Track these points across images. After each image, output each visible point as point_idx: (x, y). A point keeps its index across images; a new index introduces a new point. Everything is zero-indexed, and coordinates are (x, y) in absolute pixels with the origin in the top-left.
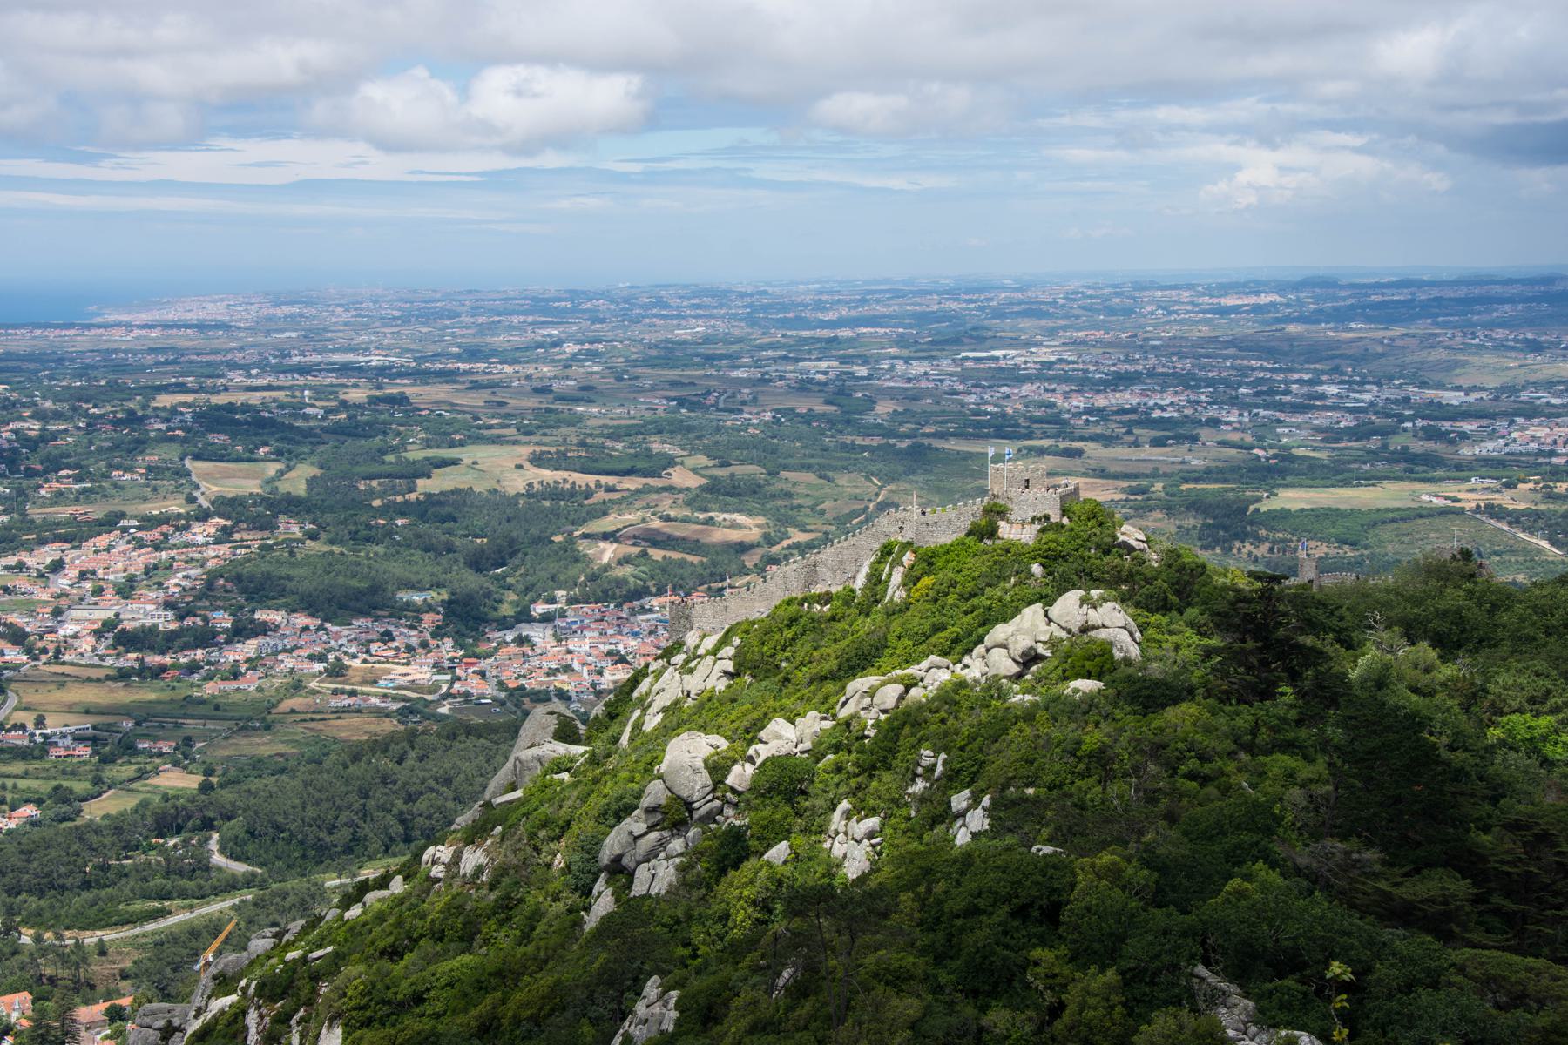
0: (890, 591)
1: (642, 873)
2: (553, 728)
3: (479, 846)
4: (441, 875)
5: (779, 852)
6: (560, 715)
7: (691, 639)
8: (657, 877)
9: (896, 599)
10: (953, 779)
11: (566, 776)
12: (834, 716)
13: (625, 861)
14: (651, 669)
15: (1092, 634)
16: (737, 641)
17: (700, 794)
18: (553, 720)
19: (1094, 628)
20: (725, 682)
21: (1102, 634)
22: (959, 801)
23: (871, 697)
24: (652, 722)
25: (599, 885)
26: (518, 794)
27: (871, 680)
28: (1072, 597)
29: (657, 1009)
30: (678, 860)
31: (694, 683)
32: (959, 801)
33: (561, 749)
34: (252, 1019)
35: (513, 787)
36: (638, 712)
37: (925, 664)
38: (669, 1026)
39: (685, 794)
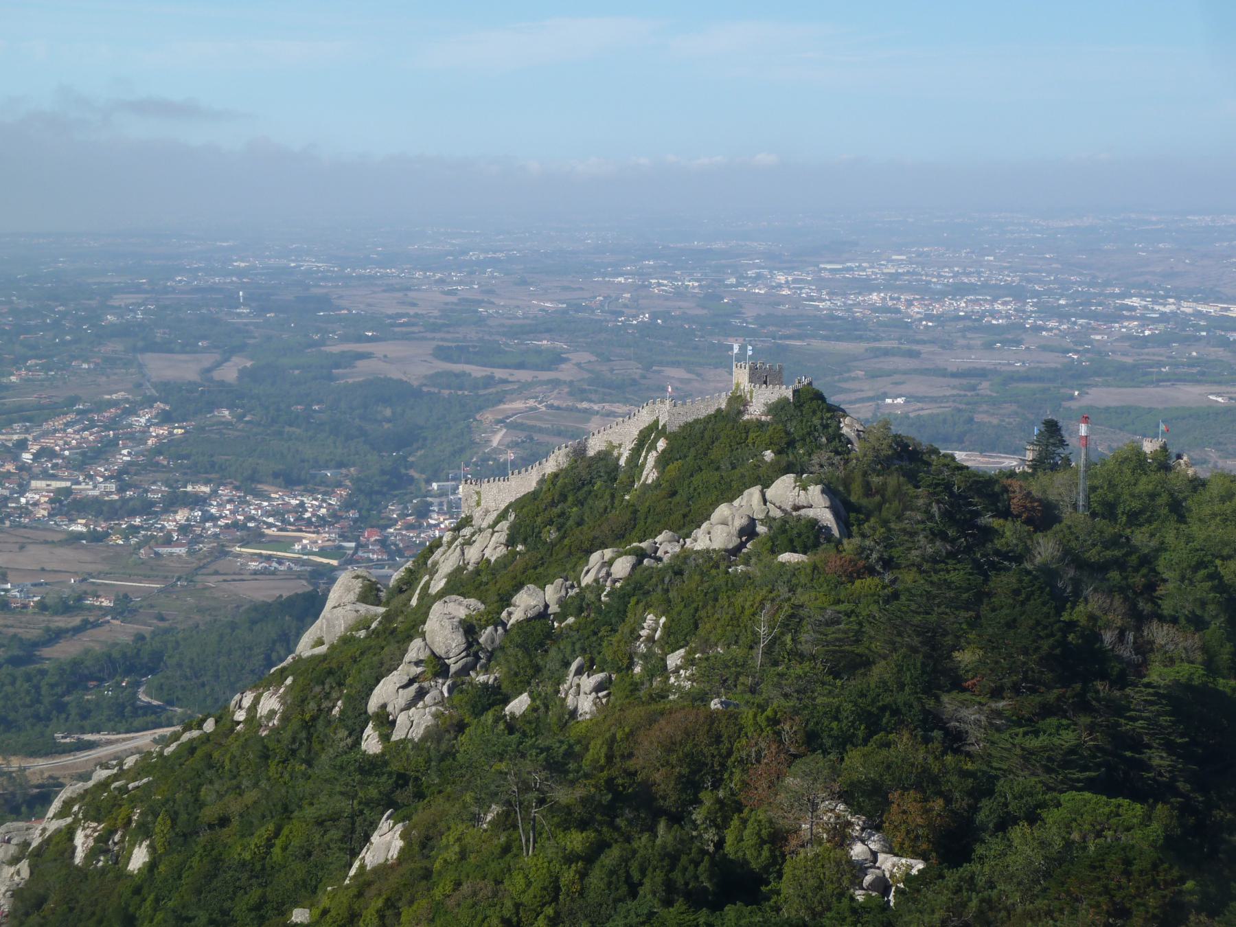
0: (645, 473)
1: (402, 719)
2: (357, 590)
3: (274, 694)
4: (242, 718)
5: (519, 704)
6: (364, 578)
7: (477, 513)
8: (414, 723)
9: (649, 481)
10: (672, 639)
11: (362, 634)
12: (579, 584)
13: (390, 709)
14: (445, 539)
15: (802, 512)
16: (512, 517)
17: (458, 651)
18: (358, 585)
19: (804, 507)
20: (503, 550)
21: (811, 513)
22: (674, 660)
23: (608, 567)
24: (438, 585)
25: (369, 730)
26: (323, 649)
27: (608, 553)
28: (789, 479)
29: (388, 837)
30: (434, 709)
31: (473, 554)
32: (674, 660)
33: (363, 608)
34: (79, 838)
35: (320, 642)
36: (426, 578)
37: (659, 539)
38: (394, 853)
39: (440, 651)
